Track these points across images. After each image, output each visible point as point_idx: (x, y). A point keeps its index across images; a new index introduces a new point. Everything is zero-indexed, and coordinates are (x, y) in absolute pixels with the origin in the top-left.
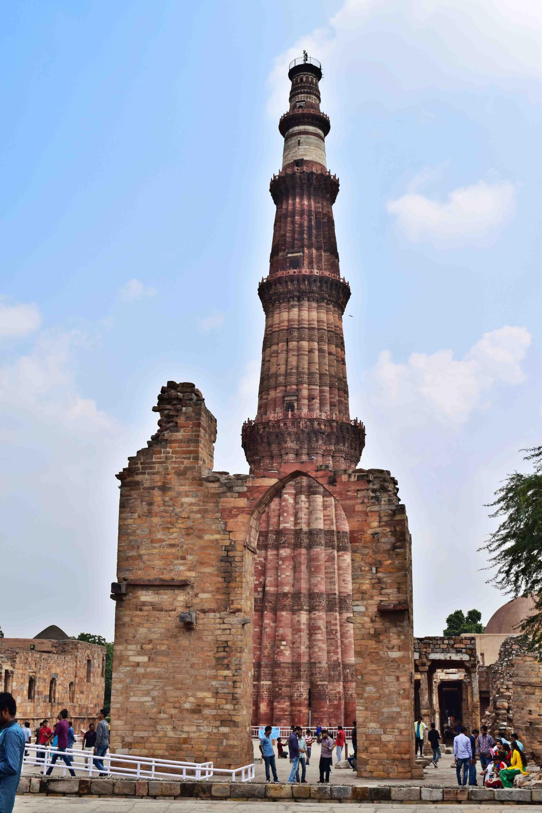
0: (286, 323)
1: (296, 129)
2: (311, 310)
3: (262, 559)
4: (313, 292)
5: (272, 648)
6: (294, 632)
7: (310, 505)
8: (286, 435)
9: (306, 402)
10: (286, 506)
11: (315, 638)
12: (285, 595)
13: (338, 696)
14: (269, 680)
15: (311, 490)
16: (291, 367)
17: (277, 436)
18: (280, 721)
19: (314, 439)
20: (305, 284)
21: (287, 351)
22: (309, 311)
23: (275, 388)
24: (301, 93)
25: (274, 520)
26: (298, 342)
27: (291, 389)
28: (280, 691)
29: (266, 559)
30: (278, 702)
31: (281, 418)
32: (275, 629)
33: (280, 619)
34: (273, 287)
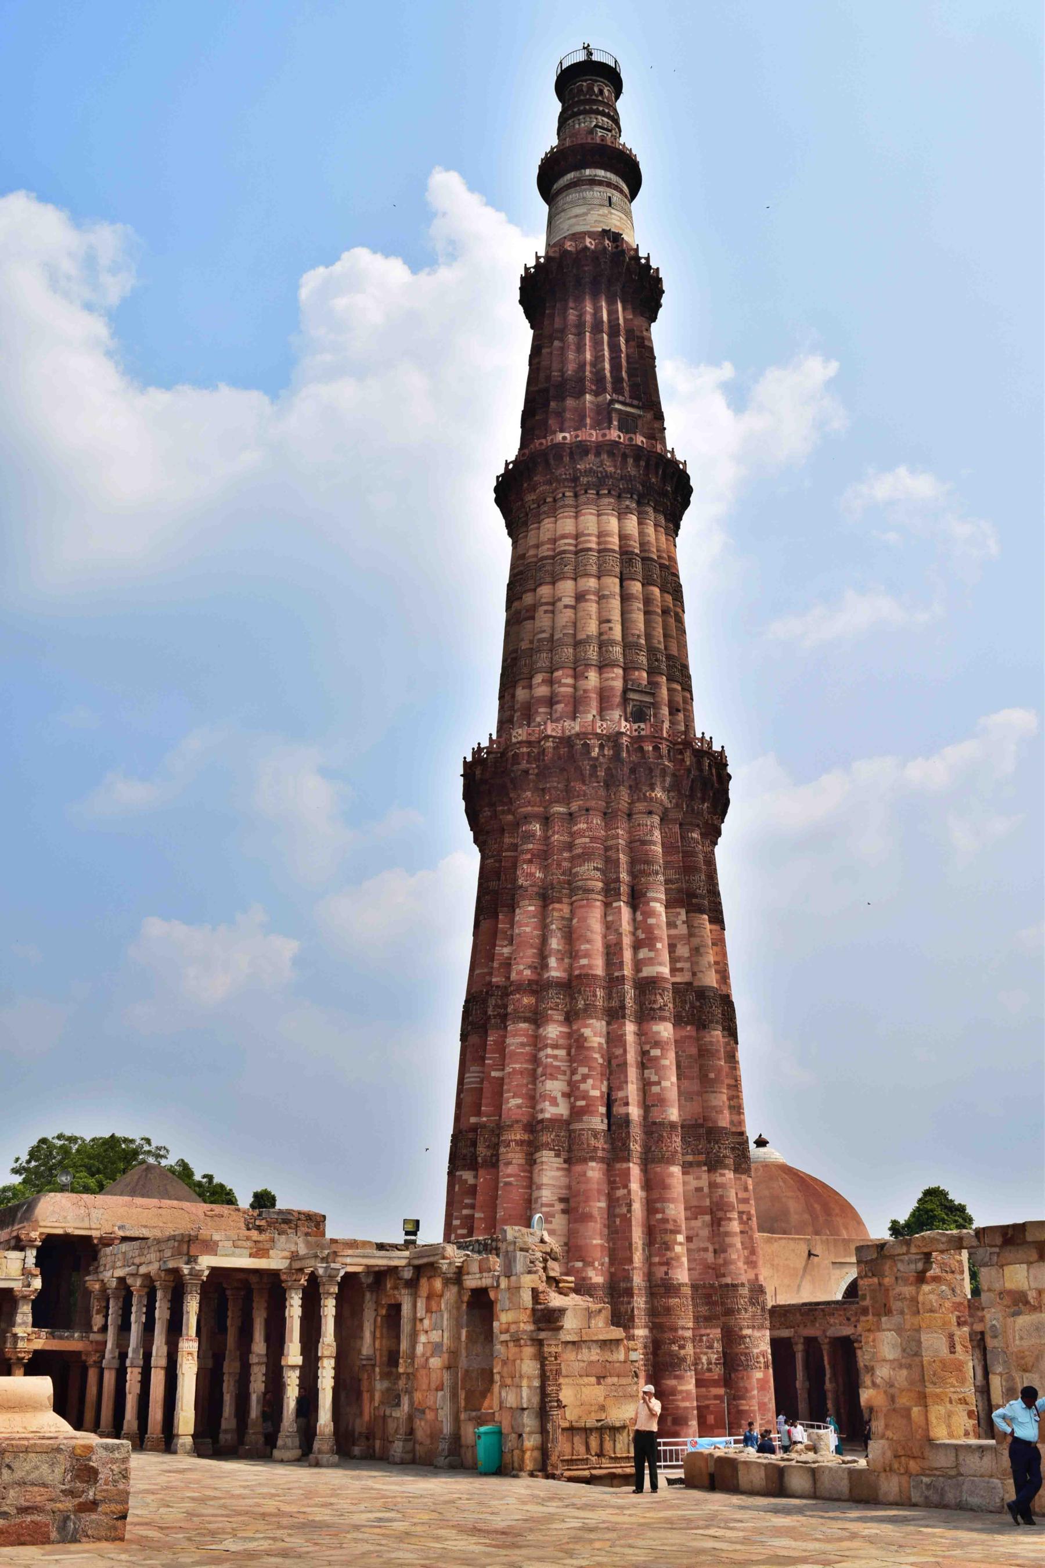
0: (616, 540)
1: (601, 173)
2: (659, 529)
3: (603, 1041)
4: (664, 494)
5: (644, 1250)
6: (689, 1213)
7: (691, 935)
8: (657, 772)
9: (665, 711)
10: (658, 926)
11: (728, 1229)
12: (673, 1126)
13: (762, 1359)
14: (645, 1327)
15: (694, 901)
16: (637, 632)
17: (633, 771)
18: (687, 1424)
19: (699, 795)
20: (657, 473)
21: (625, 598)
22: (656, 531)
23: (602, 667)
24: (603, 114)
25: (627, 955)
26: (643, 585)
27: (640, 678)
28: (683, 1352)
29: (615, 1039)
30: (677, 1377)
31: (643, 733)
32: (651, 1207)
33: (668, 1181)
34: (591, 457)
